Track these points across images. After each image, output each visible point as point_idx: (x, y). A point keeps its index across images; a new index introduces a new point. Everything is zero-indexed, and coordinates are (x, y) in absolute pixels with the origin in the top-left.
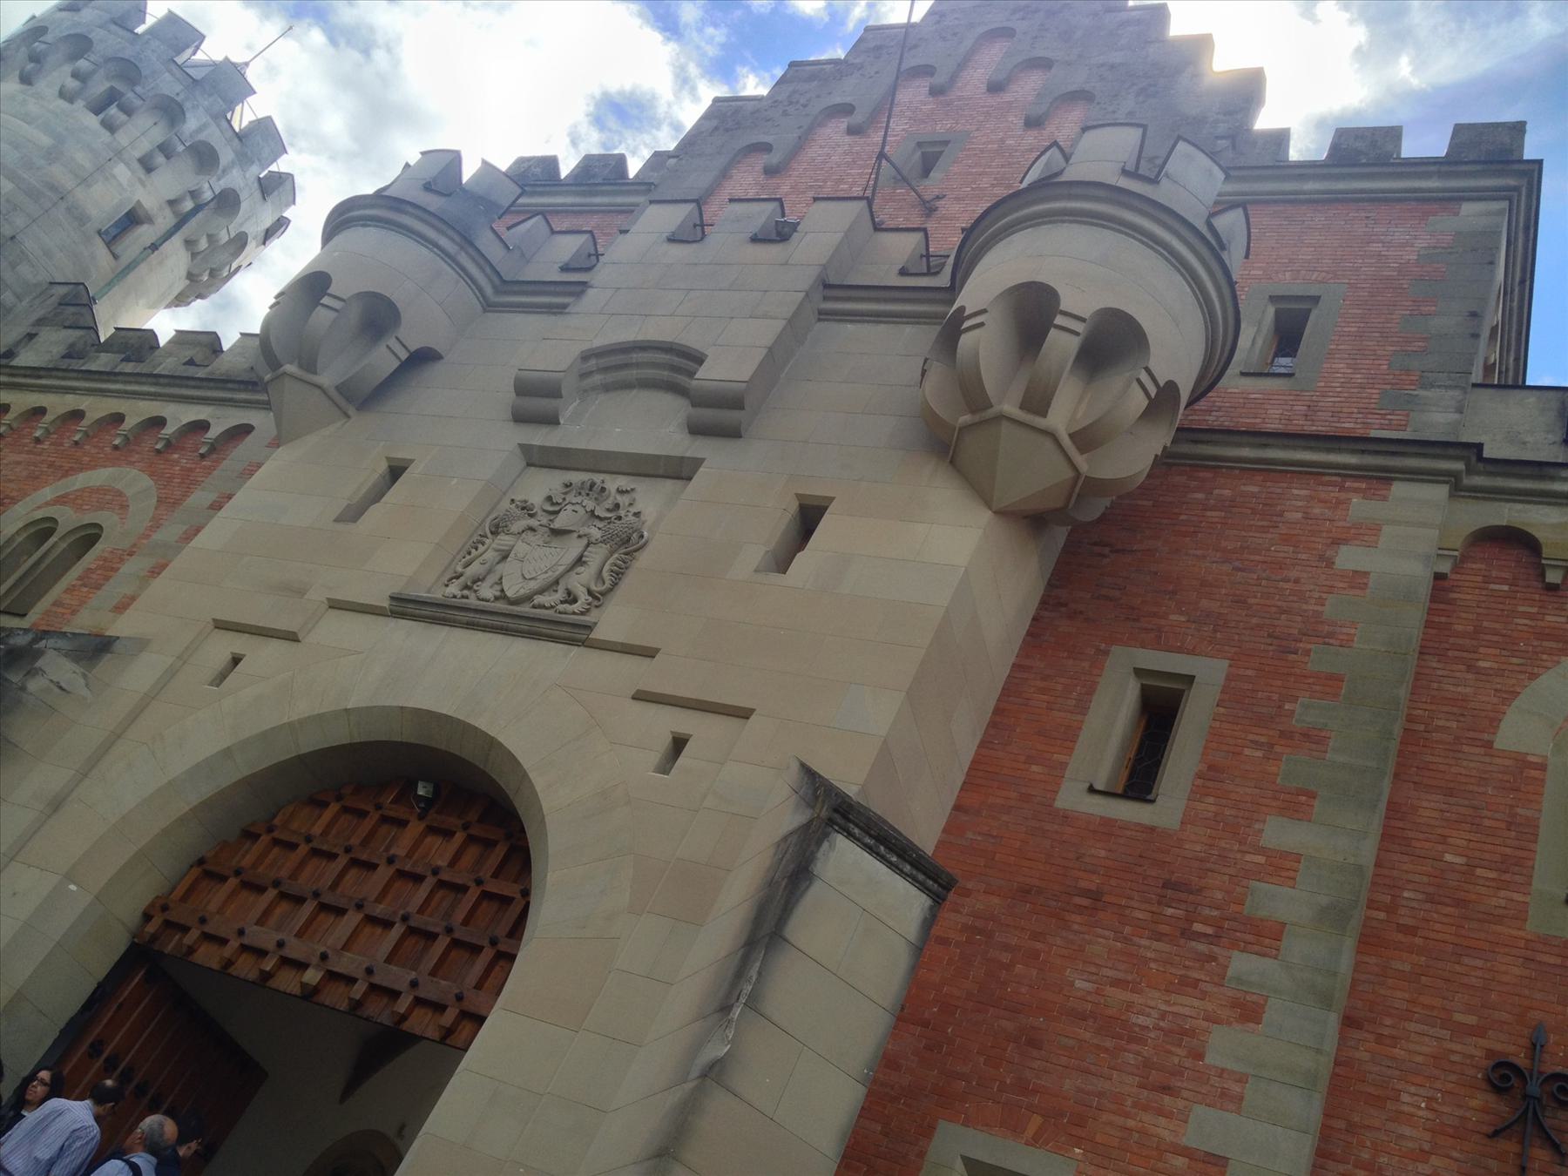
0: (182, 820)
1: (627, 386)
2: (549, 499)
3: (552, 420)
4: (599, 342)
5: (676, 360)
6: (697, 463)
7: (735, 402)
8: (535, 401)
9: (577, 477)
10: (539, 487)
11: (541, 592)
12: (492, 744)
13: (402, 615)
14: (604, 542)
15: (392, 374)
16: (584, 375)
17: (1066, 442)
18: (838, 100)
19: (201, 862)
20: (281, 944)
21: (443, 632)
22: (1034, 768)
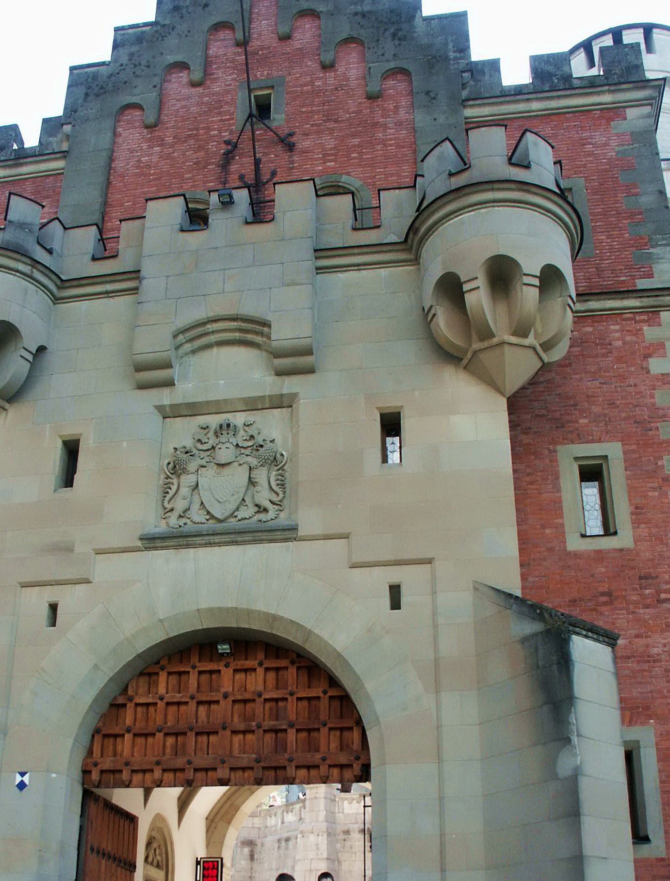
0: (87, 712)
1: (209, 346)
2: (199, 441)
3: (169, 383)
4: (182, 321)
5: (244, 325)
6: (293, 397)
7: (308, 352)
8: (150, 374)
9: (214, 420)
10: (184, 433)
11: (237, 509)
12: (275, 618)
13: (155, 548)
14: (262, 466)
15: (30, 371)
16: (177, 348)
17: (514, 340)
18: (171, 59)
19: (97, 731)
20: (189, 762)
21: (192, 551)
22: (548, 531)
